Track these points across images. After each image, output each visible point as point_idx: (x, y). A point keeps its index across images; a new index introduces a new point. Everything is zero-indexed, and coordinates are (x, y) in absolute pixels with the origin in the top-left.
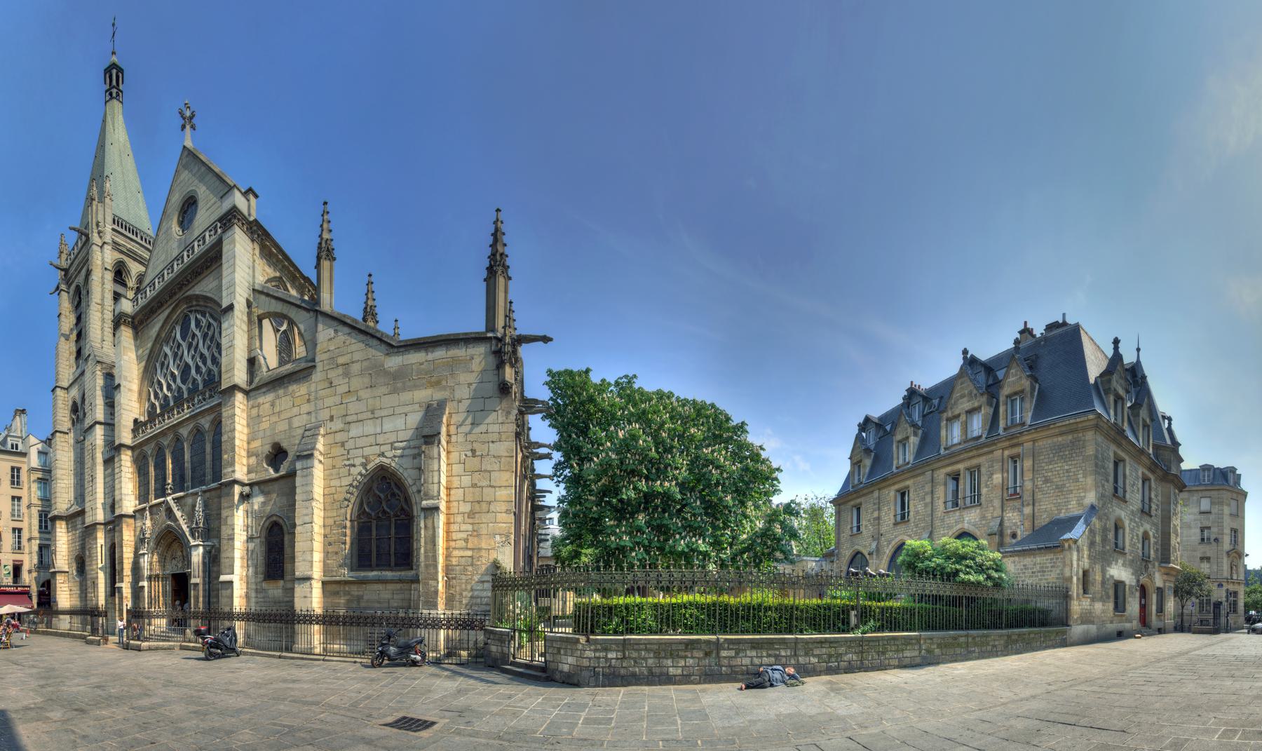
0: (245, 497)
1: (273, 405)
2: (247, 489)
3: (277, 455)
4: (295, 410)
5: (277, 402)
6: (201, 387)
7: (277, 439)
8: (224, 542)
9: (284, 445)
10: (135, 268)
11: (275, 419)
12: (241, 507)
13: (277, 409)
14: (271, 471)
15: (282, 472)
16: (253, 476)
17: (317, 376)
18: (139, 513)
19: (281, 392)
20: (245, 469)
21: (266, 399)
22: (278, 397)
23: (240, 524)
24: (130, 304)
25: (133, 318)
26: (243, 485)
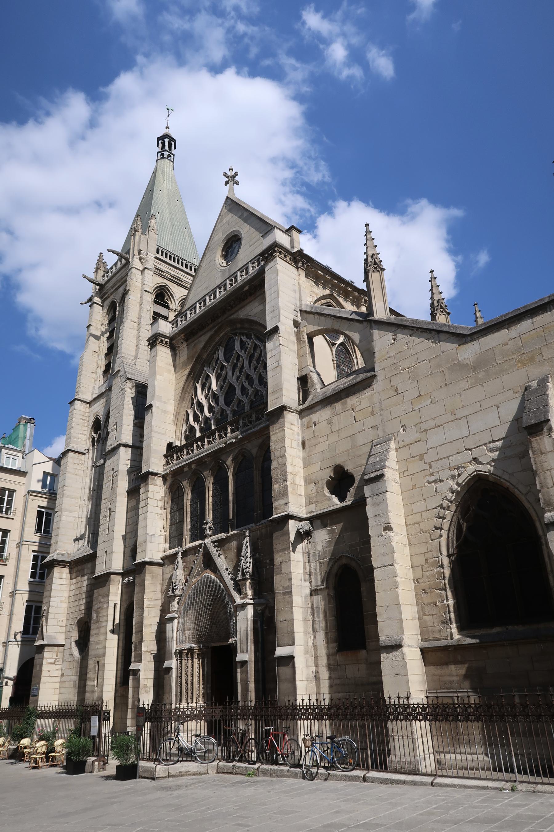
0: (302, 536)
1: (330, 422)
2: (305, 526)
3: (340, 481)
4: (358, 426)
5: (335, 418)
6: (247, 408)
7: (339, 461)
8: (279, 598)
9: (349, 468)
10: (178, 292)
11: (334, 438)
12: (300, 547)
13: (336, 428)
14: (335, 499)
15: (349, 501)
16: (313, 507)
17: (377, 386)
18: (170, 560)
19: (338, 406)
20: (303, 501)
21: (322, 415)
22: (335, 414)
23: (301, 571)
24: (169, 325)
25: (172, 339)
26: (300, 519)
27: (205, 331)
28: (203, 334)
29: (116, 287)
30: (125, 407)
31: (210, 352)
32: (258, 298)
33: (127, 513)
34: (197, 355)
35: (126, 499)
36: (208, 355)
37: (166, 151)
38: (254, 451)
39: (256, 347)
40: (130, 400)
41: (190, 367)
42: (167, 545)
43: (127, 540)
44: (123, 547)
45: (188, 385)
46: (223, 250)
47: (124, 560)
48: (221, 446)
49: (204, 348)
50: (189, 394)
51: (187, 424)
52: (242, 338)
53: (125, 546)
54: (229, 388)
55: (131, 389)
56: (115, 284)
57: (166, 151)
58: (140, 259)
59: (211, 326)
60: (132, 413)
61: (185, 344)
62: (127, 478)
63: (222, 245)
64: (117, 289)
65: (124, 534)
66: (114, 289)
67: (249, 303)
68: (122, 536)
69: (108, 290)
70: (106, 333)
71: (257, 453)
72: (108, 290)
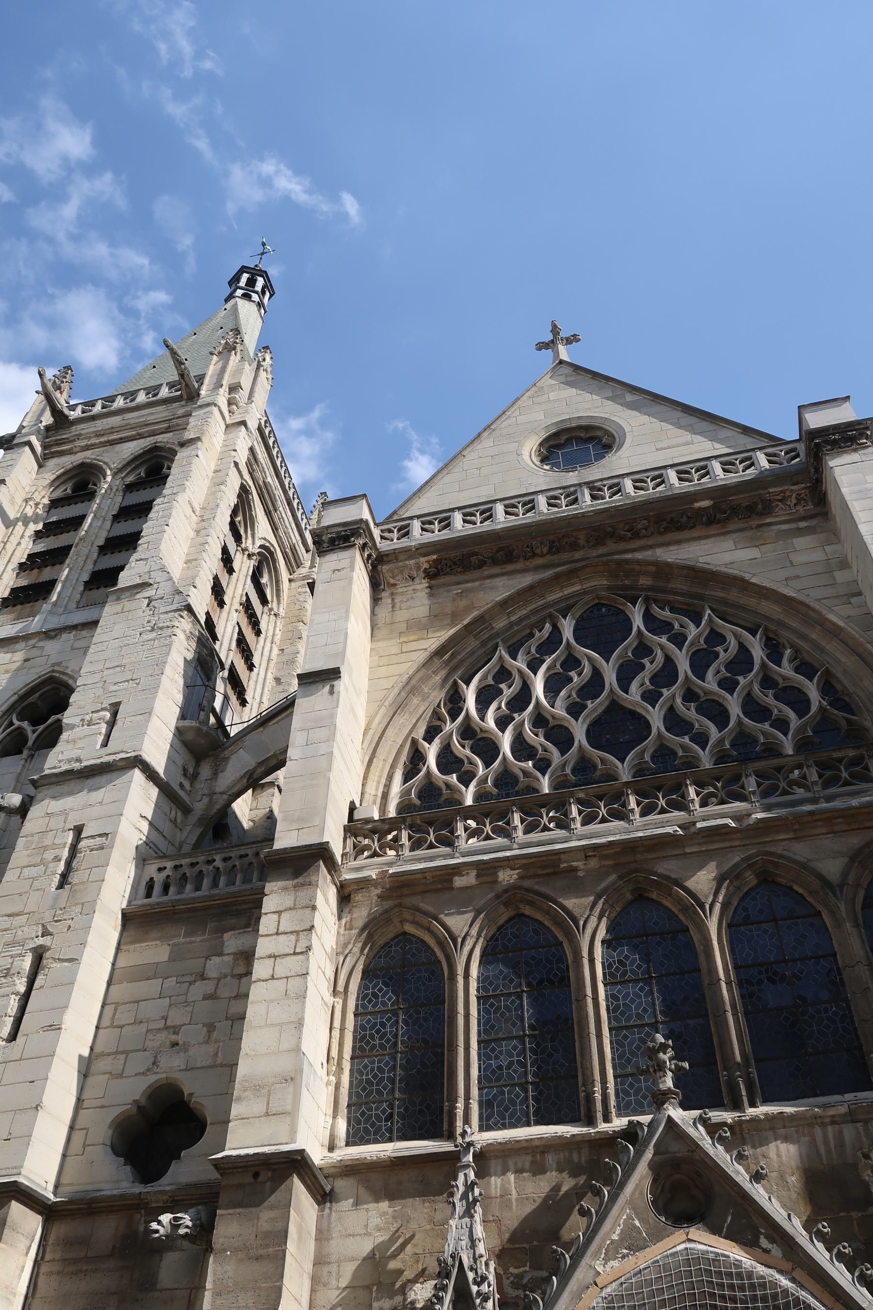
27: (510, 567)
28: (502, 575)
29: (115, 436)
30: (168, 670)
31: (521, 620)
32: (734, 536)
33: (109, 983)
34: (475, 613)
35: (115, 936)
36: (511, 625)
37: (257, 292)
38: (832, 868)
39: (716, 638)
40: (181, 664)
41: (445, 635)
42: (342, 1126)
43: (97, 1081)
44: (73, 1100)
45: (429, 677)
46: (541, 445)
47: (64, 1156)
48: (669, 830)
49: (504, 604)
50: (424, 700)
51: (408, 776)
52: (656, 610)
53: (79, 1100)
54: (607, 711)
55: (188, 638)
56: (112, 430)
57: (257, 292)
58: (230, 403)
59: (539, 561)
60: (179, 698)
61: (422, 585)
62: (130, 870)
63: (543, 435)
64: (112, 443)
65: (86, 1053)
66: (102, 439)
67: (699, 538)
68: (80, 1057)
69: (78, 437)
70: (35, 523)
71: (845, 874)
72: (78, 437)
